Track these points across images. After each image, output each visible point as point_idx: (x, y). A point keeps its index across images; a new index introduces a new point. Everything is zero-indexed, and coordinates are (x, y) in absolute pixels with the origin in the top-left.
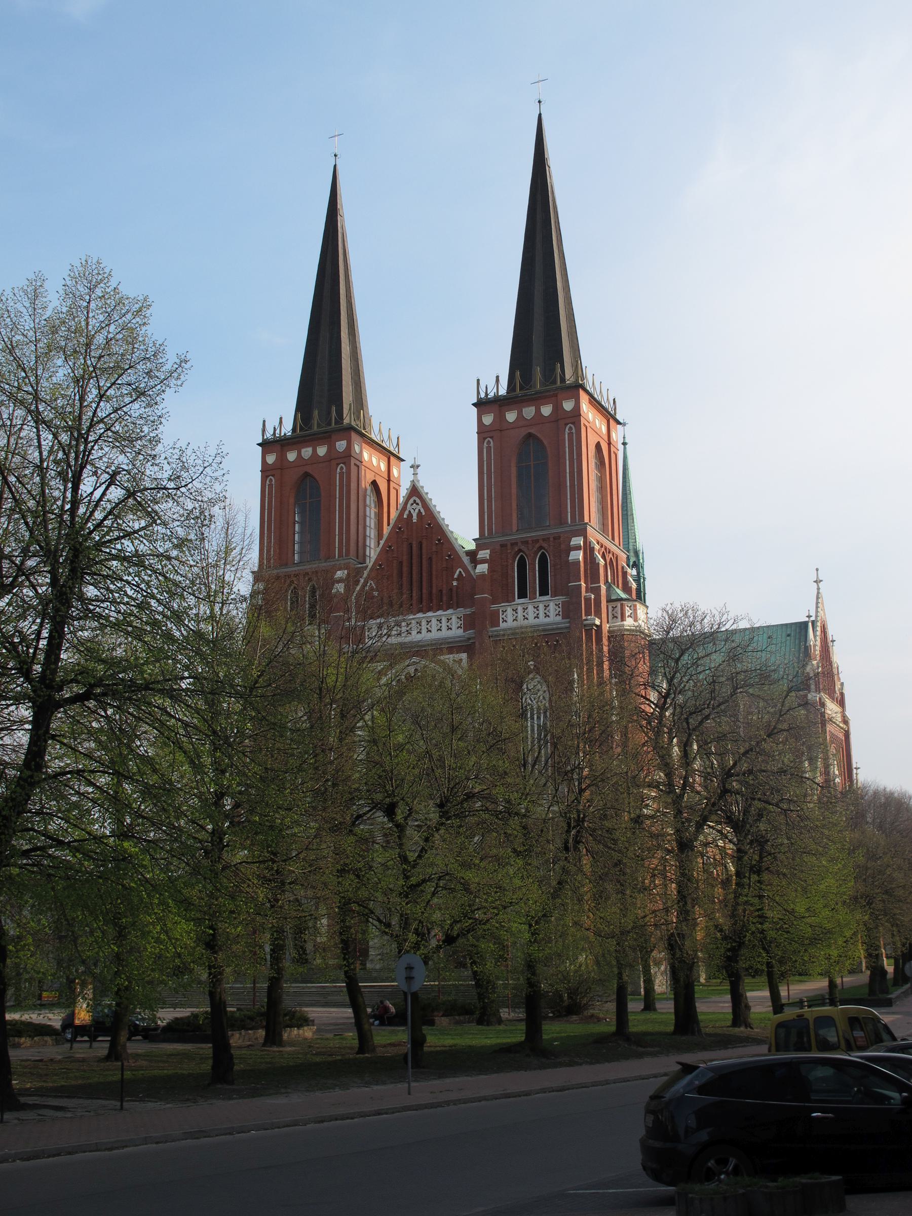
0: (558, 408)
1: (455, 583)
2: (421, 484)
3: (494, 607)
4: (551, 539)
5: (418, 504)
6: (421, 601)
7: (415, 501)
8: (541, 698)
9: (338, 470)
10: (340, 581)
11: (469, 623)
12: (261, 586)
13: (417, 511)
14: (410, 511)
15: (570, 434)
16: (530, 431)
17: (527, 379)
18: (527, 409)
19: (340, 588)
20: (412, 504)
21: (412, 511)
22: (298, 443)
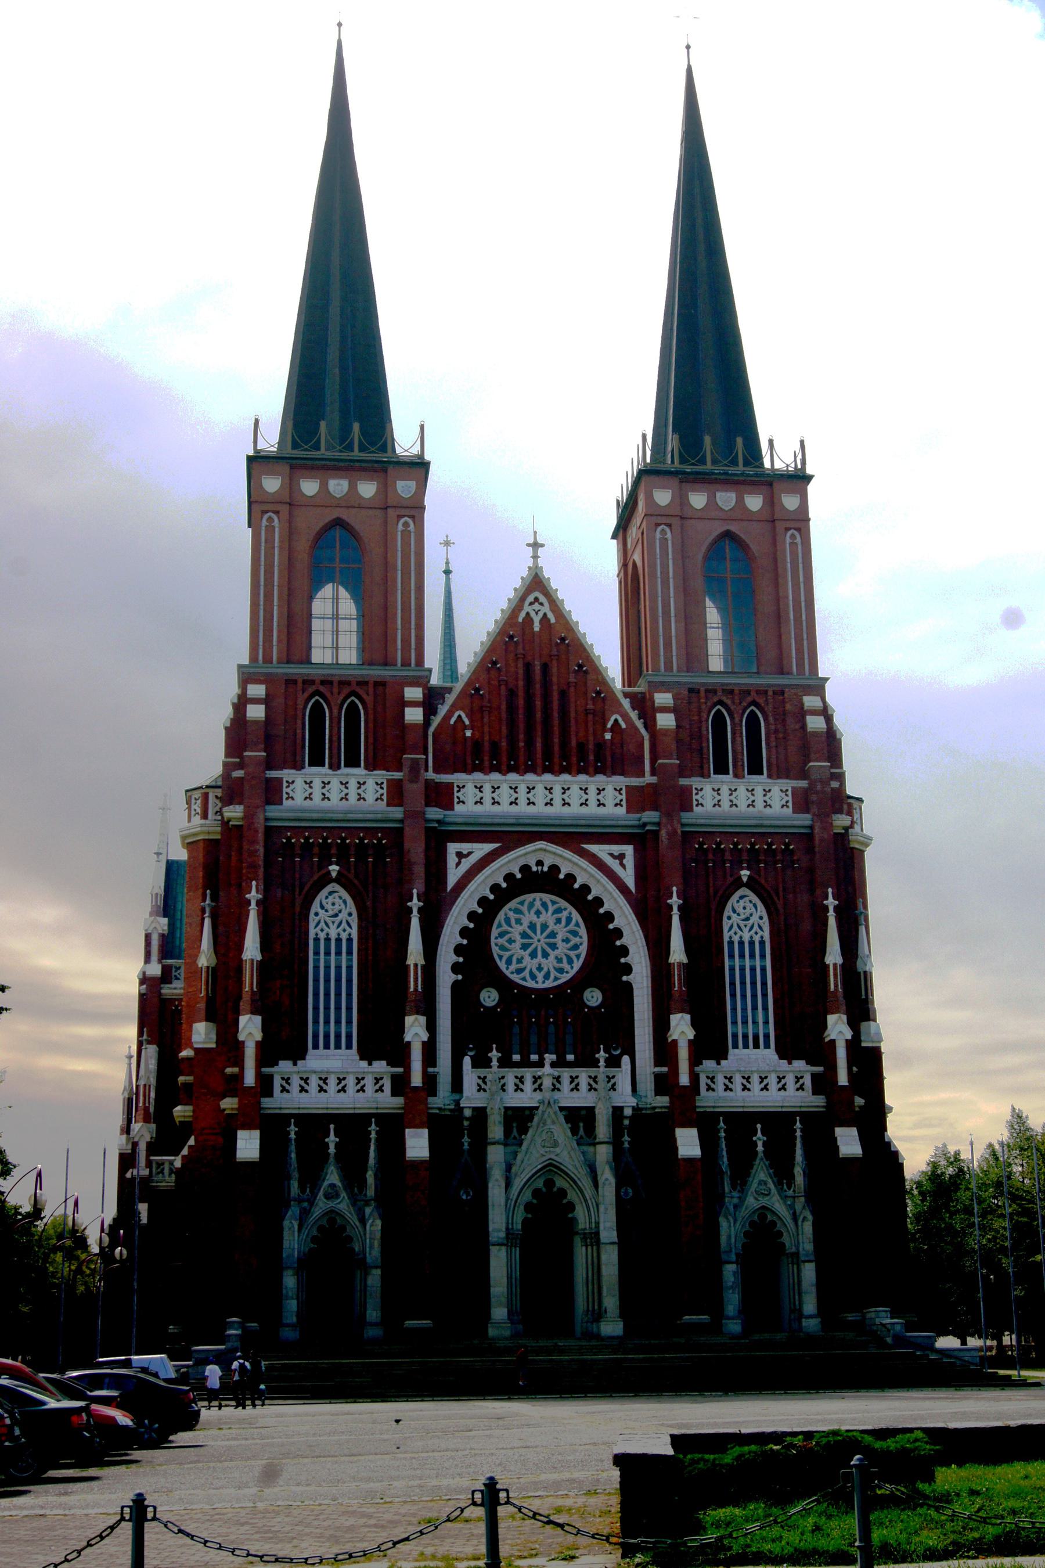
0: (771, 502)
1: (608, 736)
2: (546, 574)
3: (683, 781)
4: (770, 693)
5: (541, 604)
6: (548, 754)
7: (536, 599)
8: (756, 927)
9: (400, 527)
10: (414, 704)
11: (637, 800)
12: (257, 690)
13: (541, 614)
14: (528, 614)
15: (793, 544)
16: (728, 528)
17: (690, 448)
18: (723, 494)
19: (414, 715)
20: (531, 604)
21: (533, 614)
22: (325, 468)
